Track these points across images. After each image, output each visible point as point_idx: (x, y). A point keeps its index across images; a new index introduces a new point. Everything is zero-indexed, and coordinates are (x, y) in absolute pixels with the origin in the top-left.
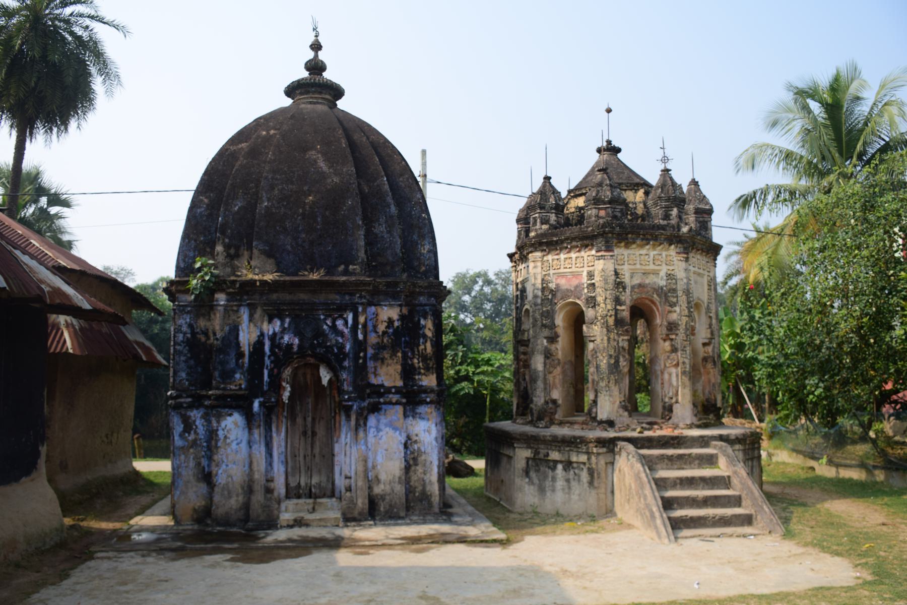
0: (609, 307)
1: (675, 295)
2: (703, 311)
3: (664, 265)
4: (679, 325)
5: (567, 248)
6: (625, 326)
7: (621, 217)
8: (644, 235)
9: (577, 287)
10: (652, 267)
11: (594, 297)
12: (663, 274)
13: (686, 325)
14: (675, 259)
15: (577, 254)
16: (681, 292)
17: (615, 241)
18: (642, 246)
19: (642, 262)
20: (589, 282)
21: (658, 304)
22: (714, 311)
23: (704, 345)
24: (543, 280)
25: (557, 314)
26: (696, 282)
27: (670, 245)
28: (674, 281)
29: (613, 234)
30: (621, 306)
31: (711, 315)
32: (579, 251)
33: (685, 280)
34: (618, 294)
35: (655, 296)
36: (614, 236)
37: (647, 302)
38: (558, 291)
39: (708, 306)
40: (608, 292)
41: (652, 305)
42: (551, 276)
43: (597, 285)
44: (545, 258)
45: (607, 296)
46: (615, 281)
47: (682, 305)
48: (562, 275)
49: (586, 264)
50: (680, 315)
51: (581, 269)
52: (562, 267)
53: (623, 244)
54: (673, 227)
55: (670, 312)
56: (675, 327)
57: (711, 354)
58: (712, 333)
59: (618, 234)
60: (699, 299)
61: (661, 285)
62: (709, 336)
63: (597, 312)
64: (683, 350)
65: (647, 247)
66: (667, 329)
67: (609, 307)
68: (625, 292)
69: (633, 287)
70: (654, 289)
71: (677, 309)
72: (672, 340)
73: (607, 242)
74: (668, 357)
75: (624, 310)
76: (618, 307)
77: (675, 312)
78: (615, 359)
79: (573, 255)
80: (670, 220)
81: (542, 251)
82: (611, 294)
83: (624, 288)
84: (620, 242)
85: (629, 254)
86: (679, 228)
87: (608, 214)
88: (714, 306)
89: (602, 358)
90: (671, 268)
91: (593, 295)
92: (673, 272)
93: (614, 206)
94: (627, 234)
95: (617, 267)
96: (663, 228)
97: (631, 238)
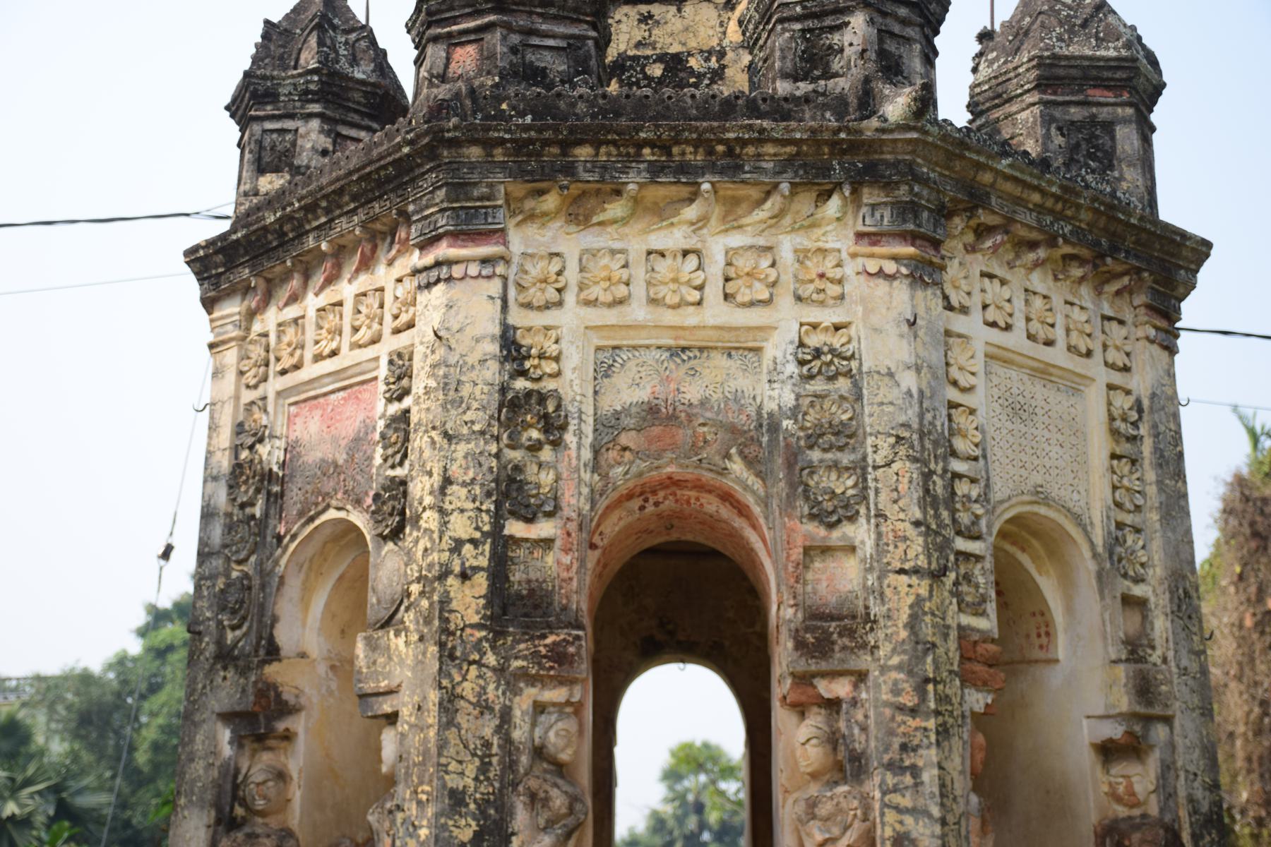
0: (461, 527)
1: (846, 459)
2: (1086, 567)
3: (785, 302)
4: (867, 618)
5: (323, 256)
6: (551, 628)
7: (567, 80)
8: (664, 147)
9: (358, 441)
10: (716, 313)
11: (404, 483)
12: (779, 348)
13: (913, 624)
14: (850, 269)
15: (364, 282)
16: (885, 444)
17: (504, 185)
18: (662, 213)
19: (663, 291)
20: (394, 408)
21: (757, 510)
22: (1157, 572)
23: (1108, 752)
24: (240, 426)
25: (293, 586)
26: (1018, 410)
27: (825, 196)
28: (843, 384)
29: (489, 145)
30: (530, 520)
31: (1138, 591)
32: (366, 264)
33: (909, 381)
34: (516, 455)
35: (737, 467)
36: (499, 154)
37: (712, 505)
38: (292, 476)
39: (1115, 542)
40: (462, 448)
41: (739, 523)
42: (270, 408)
43: (414, 418)
44: (257, 327)
45: (455, 470)
46: (503, 390)
47: (891, 511)
48: (305, 396)
49: (388, 318)
50: (878, 566)
51: (370, 352)
52: (308, 355)
53: (551, 201)
54: (839, 105)
55: (815, 551)
56: (850, 633)
57: (1153, 810)
58: (1144, 688)
59: (520, 147)
60: (1040, 495)
61: (770, 406)
62: (1124, 703)
63: (410, 559)
64: (893, 767)
65: (691, 212)
66: (800, 645)
67: (461, 527)
68: (557, 444)
69: (608, 426)
70: (733, 430)
71: (861, 532)
72: (833, 705)
73: (459, 189)
74: (812, 804)
75: (547, 543)
76: (515, 528)
77: (852, 549)
78: (482, 813)
79: (346, 290)
80: (828, 75)
81: (247, 290)
82: (475, 459)
83: (554, 427)
84: (541, 193)
85: (594, 253)
86: (867, 102)
87: (492, 56)
88: (1156, 545)
89: (413, 809)
90: (828, 317)
91: (399, 472)
92: (837, 341)
93: (522, 21)
94: (566, 146)
95: (517, 317)
96: (782, 109)
97: (594, 165)
